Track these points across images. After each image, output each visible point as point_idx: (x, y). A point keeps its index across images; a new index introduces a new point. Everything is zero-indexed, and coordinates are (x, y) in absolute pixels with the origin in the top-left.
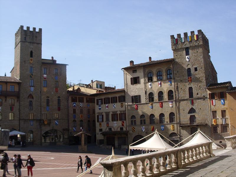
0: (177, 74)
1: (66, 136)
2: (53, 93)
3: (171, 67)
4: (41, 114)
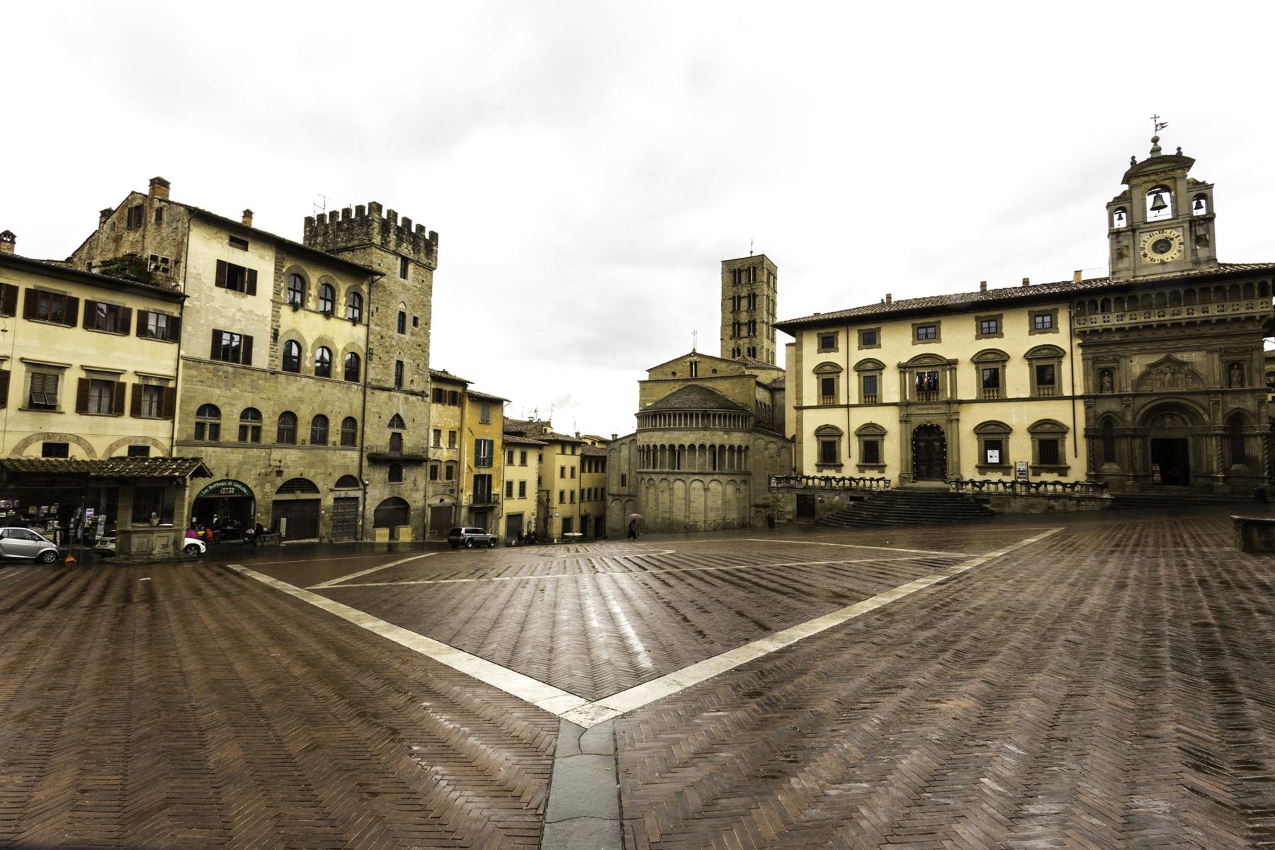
0: (375, 314)
3: (362, 290)
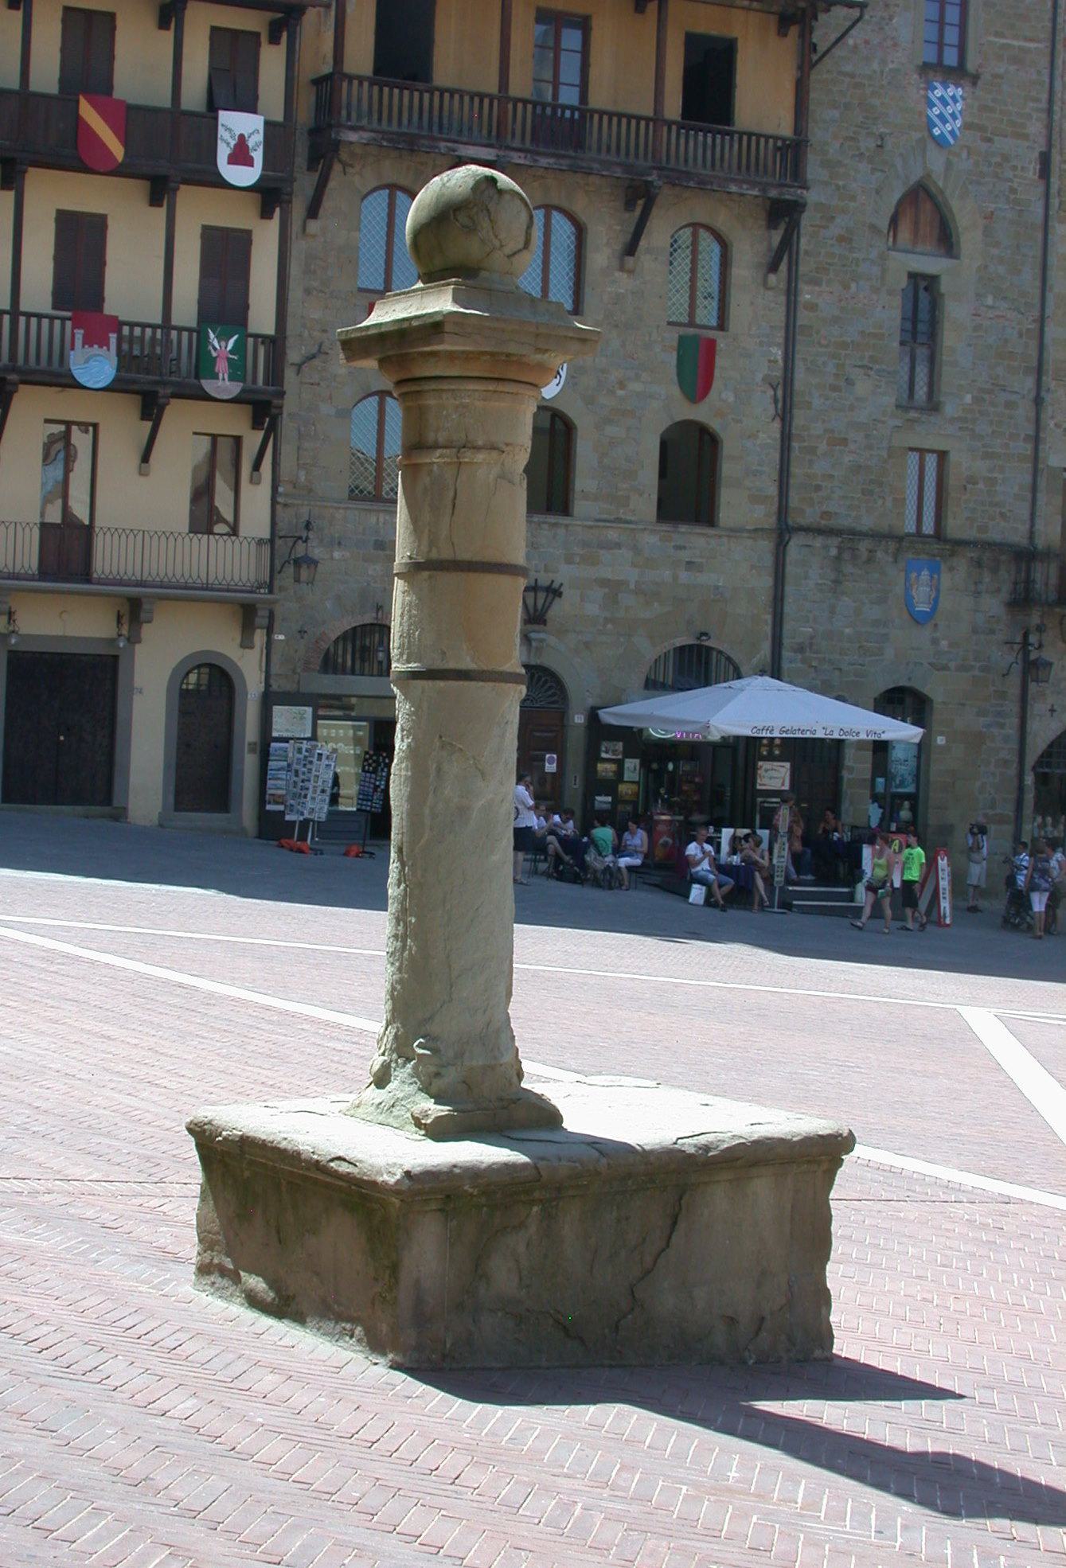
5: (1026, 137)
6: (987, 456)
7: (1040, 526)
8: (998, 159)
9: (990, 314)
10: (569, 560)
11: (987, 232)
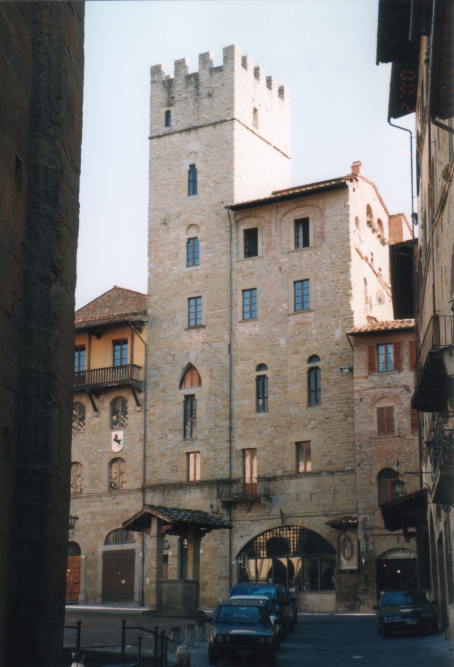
1: (349, 559)
2: (282, 342)
4: (231, 453)
5: (223, 341)
6: (213, 450)
7: (234, 471)
8: (214, 351)
9: (213, 402)
10: (81, 508)
11: (211, 376)
